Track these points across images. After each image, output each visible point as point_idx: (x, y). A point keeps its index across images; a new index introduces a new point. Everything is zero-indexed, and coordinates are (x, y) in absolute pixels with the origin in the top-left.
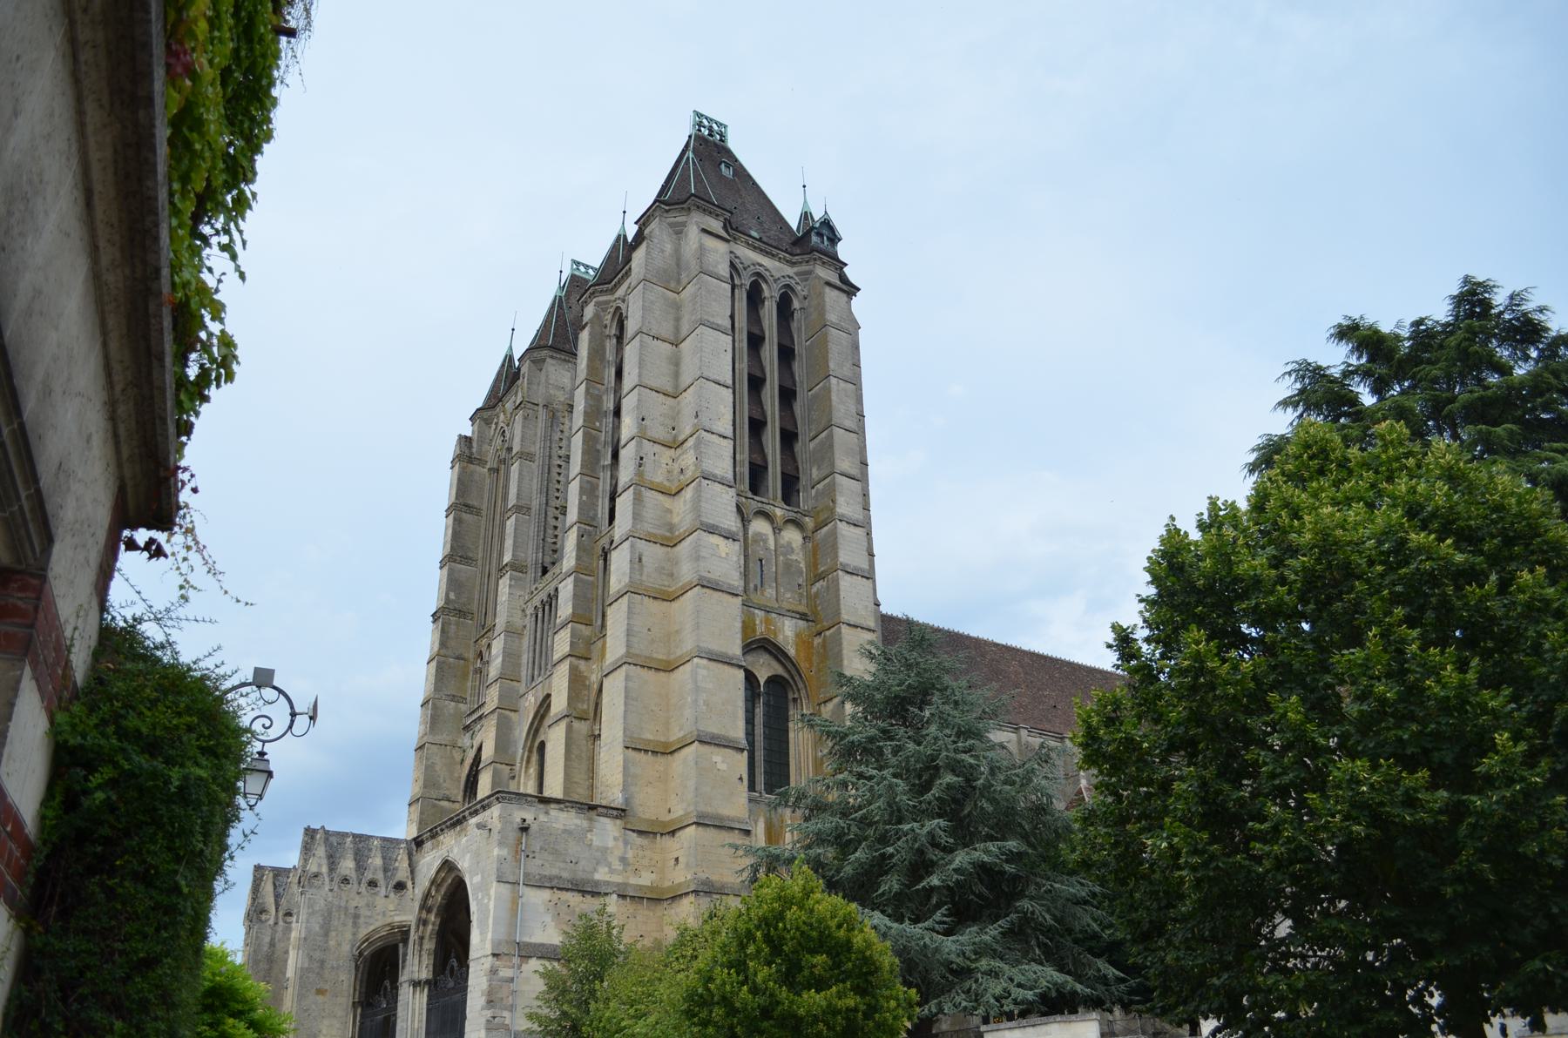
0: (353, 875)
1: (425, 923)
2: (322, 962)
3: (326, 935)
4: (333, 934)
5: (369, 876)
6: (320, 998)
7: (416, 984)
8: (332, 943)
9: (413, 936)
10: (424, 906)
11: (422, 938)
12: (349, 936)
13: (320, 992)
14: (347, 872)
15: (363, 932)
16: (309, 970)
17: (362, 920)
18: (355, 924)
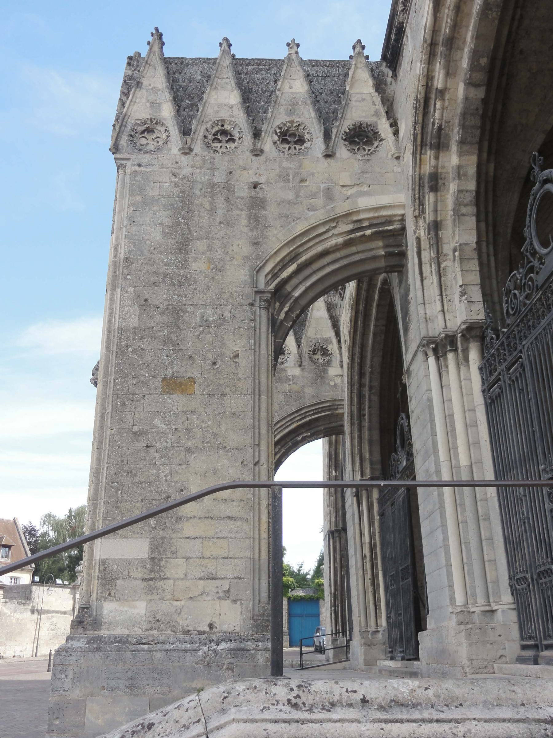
0: (239, 119)
1: (435, 182)
2: (176, 313)
3: (183, 247)
4: (200, 245)
5: (280, 117)
6: (176, 402)
7: (442, 346)
8: (198, 266)
9: (415, 231)
10: (430, 139)
11: (436, 227)
12: (241, 247)
13: (174, 385)
14: (224, 114)
15: (277, 238)
16: (141, 332)
17: (271, 212)
18: (256, 221)
